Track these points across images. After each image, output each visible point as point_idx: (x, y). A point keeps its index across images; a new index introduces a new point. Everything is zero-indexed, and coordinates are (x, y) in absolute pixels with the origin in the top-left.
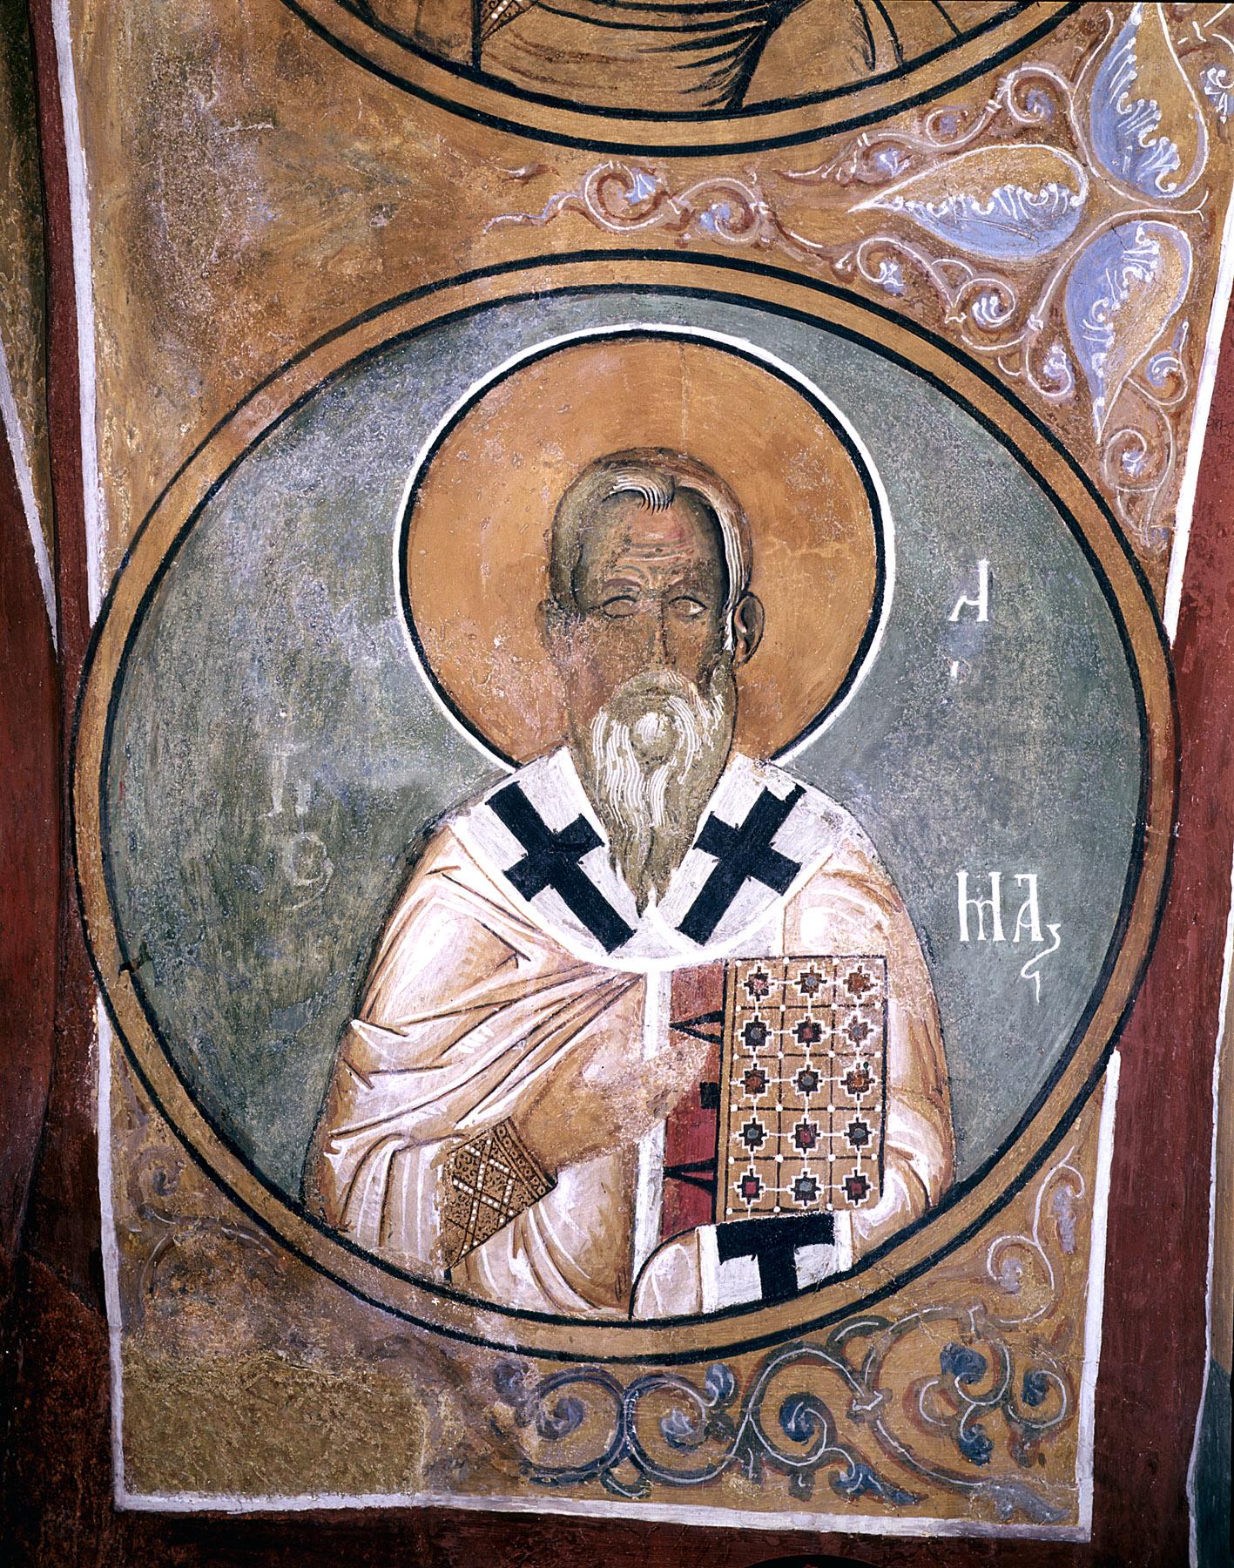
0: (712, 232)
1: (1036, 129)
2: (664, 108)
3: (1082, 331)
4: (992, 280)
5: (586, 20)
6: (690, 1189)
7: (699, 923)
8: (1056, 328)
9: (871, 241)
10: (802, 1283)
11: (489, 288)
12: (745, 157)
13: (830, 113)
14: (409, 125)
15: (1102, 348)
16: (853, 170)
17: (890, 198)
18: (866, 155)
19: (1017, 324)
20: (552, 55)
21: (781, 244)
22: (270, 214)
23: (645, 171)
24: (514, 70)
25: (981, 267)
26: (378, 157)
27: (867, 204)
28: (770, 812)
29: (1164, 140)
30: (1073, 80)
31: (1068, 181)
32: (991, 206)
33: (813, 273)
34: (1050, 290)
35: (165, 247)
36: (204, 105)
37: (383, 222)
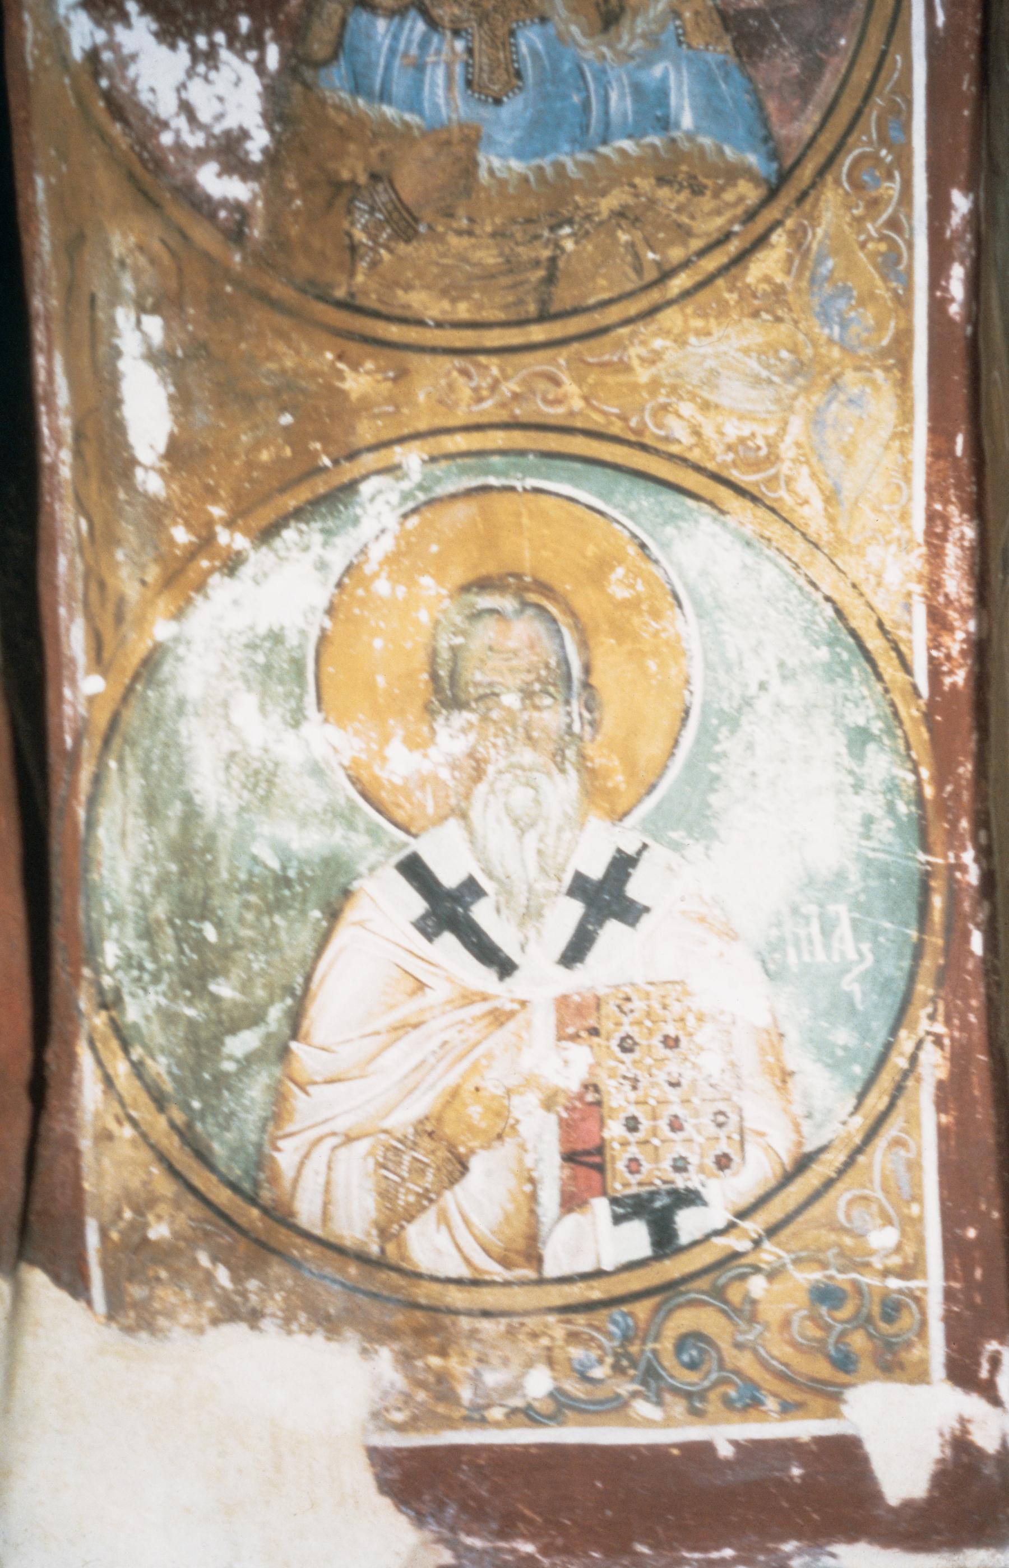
6: (582, 1171)
7: (575, 953)
10: (684, 1239)
28: (623, 865)
33: (616, 428)
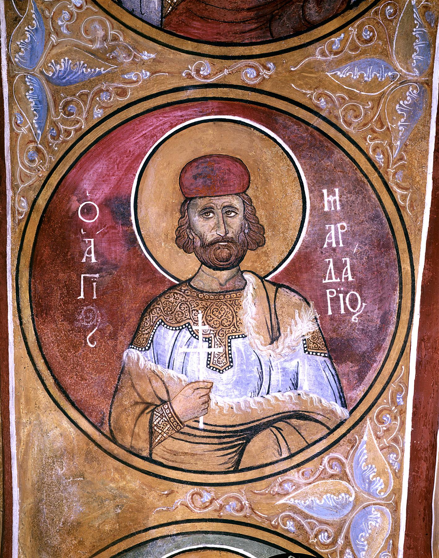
0: (230, 512)
1: (336, 475)
2: (213, 470)
3: (356, 545)
4: (325, 527)
5: (187, 441)
8: (348, 543)
9: (283, 514)
11: (154, 533)
12: (240, 486)
13: (268, 471)
14: (128, 478)
15: (363, 550)
16: (276, 490)
17: (289, 499)
18: (280, 485)
19: (334, 542)
20: (175, 453)
21: (254, 516)
22: (81, 509)
23: (207, 491)
24: (163, 458)
25: (321, 522)
26: (118, 488)
27: (282, 501)
29: (378, 478)
30: (347, 458)
31: (348, 492)
32: (323, 501)
33: (265, 525)
34: (344, 531)
35: (45, 521)
36: (60, 472)
37: (119, 511)
